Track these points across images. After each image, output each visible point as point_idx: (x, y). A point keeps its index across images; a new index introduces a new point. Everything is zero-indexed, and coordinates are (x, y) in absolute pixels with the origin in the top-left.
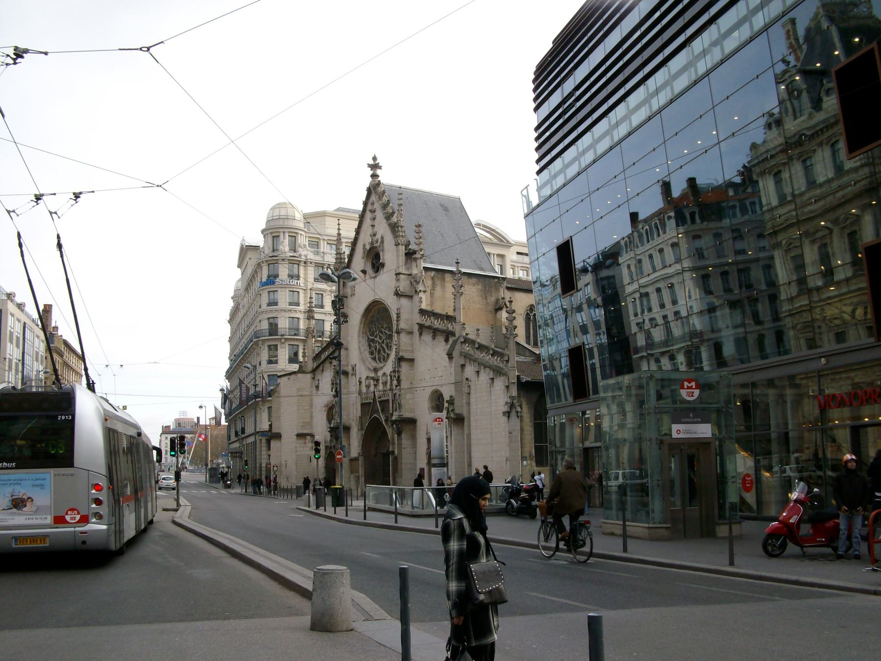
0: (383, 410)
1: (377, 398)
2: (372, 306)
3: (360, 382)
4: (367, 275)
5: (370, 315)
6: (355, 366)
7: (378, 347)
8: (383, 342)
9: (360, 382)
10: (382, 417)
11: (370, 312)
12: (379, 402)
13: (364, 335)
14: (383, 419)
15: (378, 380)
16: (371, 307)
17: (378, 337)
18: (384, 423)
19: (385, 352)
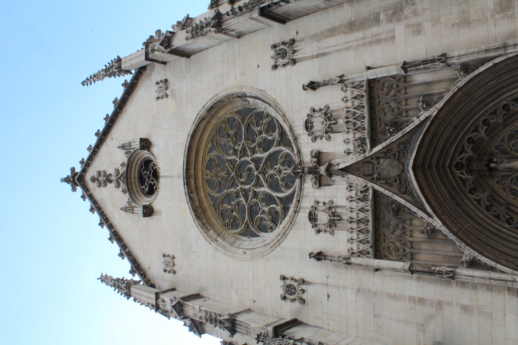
0: (397, 126)
1: (361, 157)
2: (194, 195)
3: (319, 256)
4: (156, 206)
5: (211, 213)
6: (284, 278)
7: (265, 189)
8: (257, 161)
9: (319, 256)
10: (417, 122)
11: (204, 211)
12: (372, 147)
13: (238, 243)
14: (424, 115)
15: (318, 156)
16: (197, 203)
17: (247, 187)
18: (433, 111)
19: (273, 158)
